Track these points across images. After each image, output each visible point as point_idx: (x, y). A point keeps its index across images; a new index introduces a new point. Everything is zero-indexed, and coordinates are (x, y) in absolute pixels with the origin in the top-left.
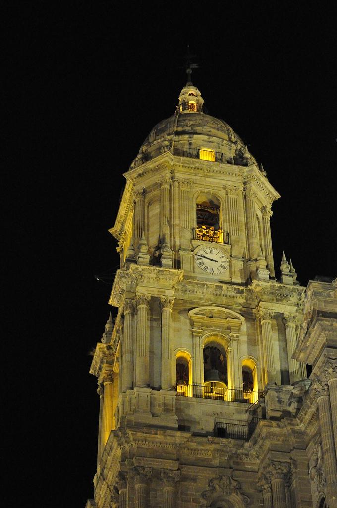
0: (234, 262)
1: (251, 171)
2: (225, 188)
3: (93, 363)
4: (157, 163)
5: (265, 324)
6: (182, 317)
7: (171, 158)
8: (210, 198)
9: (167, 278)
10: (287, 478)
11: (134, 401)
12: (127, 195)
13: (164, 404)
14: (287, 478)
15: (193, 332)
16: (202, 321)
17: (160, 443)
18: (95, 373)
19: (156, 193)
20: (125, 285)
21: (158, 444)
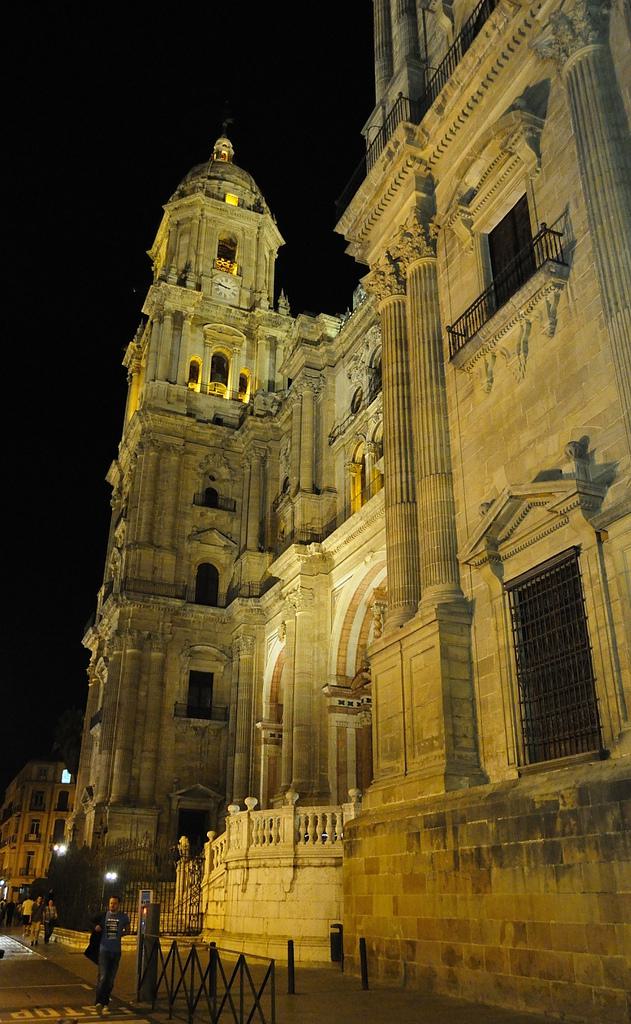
0: (243, 291)
1: (266, 218)
6: (198, 330)
10: (263, 460)
14: (263, 460)
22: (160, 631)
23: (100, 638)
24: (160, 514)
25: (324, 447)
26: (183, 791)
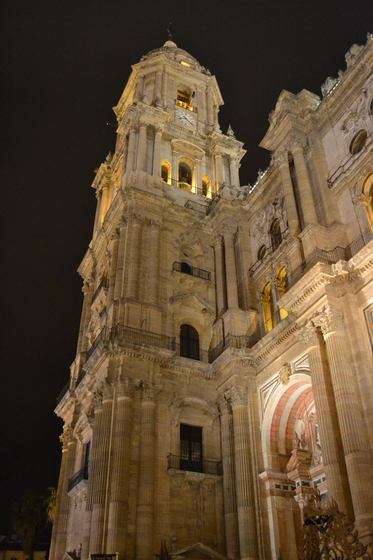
0: (199, 123)
1: (212, 79)
2: (195, 85)
3: (95, 179)
4: (155, 61)
5: (218, 158)
7: (164, 59)
8: (185, 89)
9: (160, 116)
11: (134, 178)
12: (131, 82)
13: (155, 184)
15: (173, 152)
16: (179, 147)
17: (152, 204)
18: (95, 186)
19: (152, 78)
20: (132, 116)
21: (150, 204)
22: (151, 381)
23: (76, 402)
24: (144, 276)
25: (322, 191)
26: (183, 551)
